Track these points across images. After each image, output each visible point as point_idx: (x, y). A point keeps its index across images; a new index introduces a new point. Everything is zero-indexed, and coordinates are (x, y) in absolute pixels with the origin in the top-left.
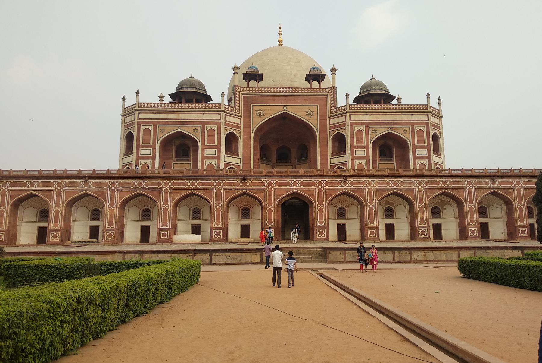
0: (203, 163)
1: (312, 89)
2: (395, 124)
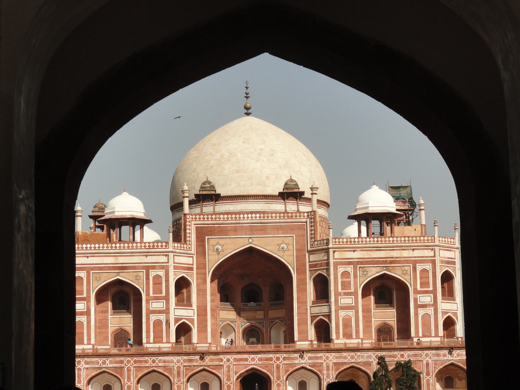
0: (148, 319)
1: (286, 215)
2: (391, 262)
